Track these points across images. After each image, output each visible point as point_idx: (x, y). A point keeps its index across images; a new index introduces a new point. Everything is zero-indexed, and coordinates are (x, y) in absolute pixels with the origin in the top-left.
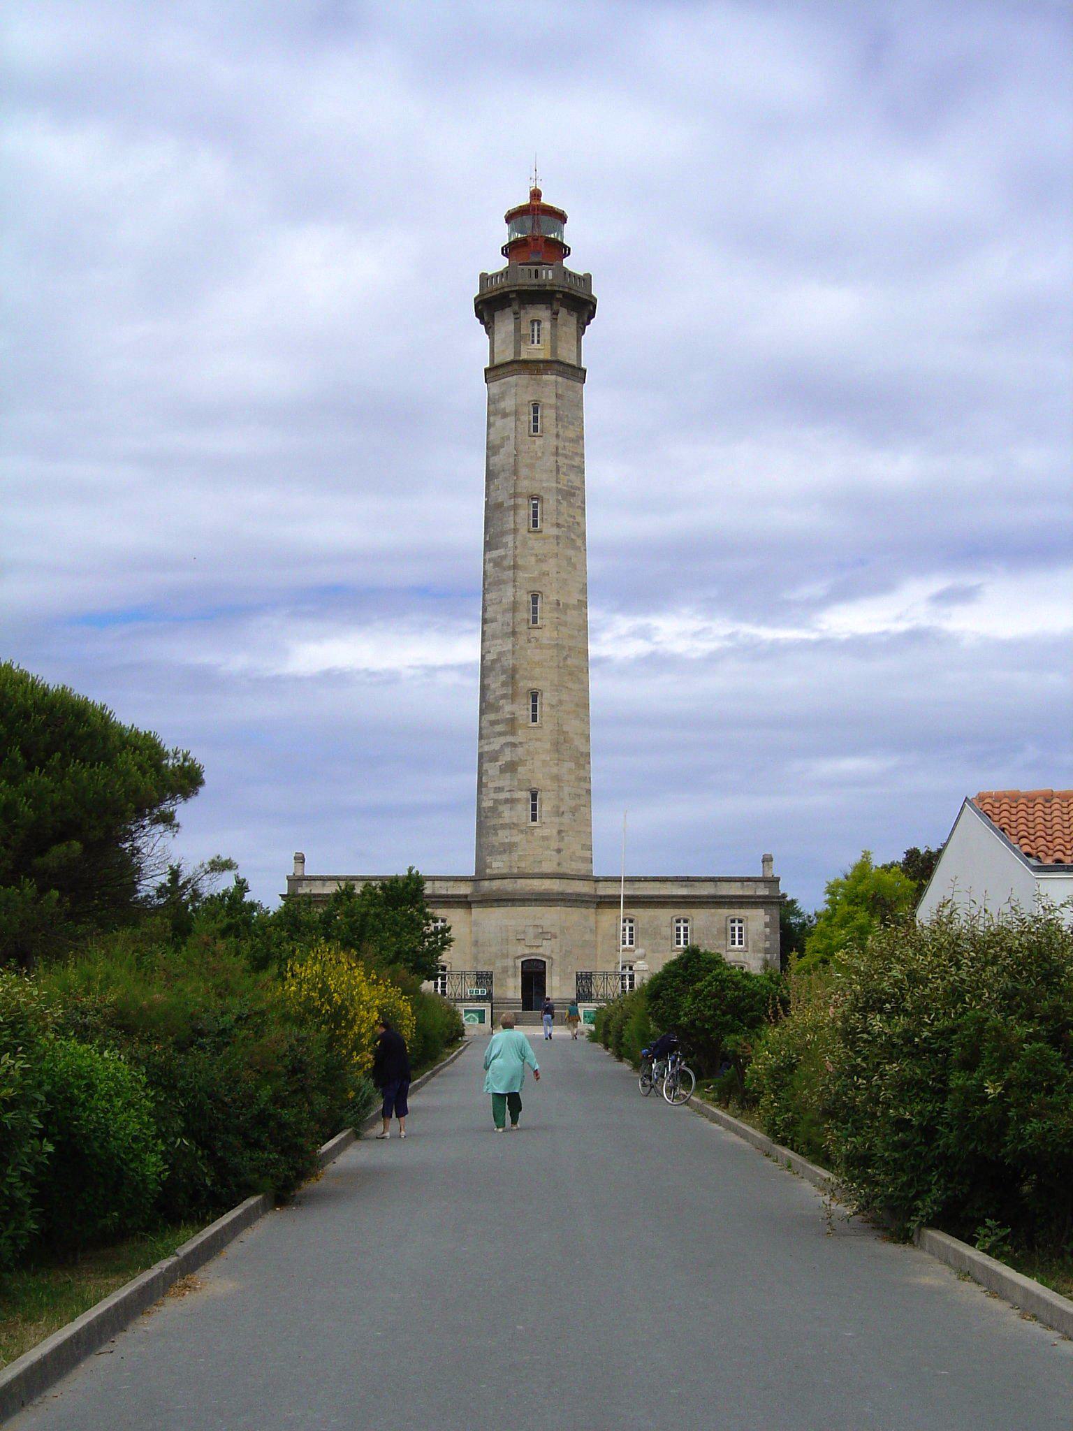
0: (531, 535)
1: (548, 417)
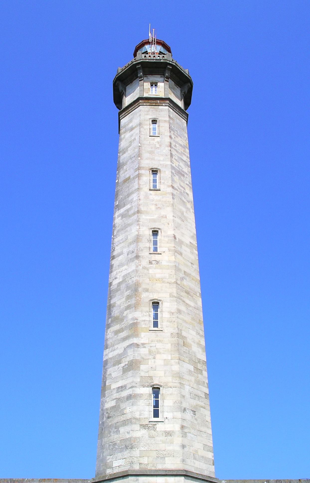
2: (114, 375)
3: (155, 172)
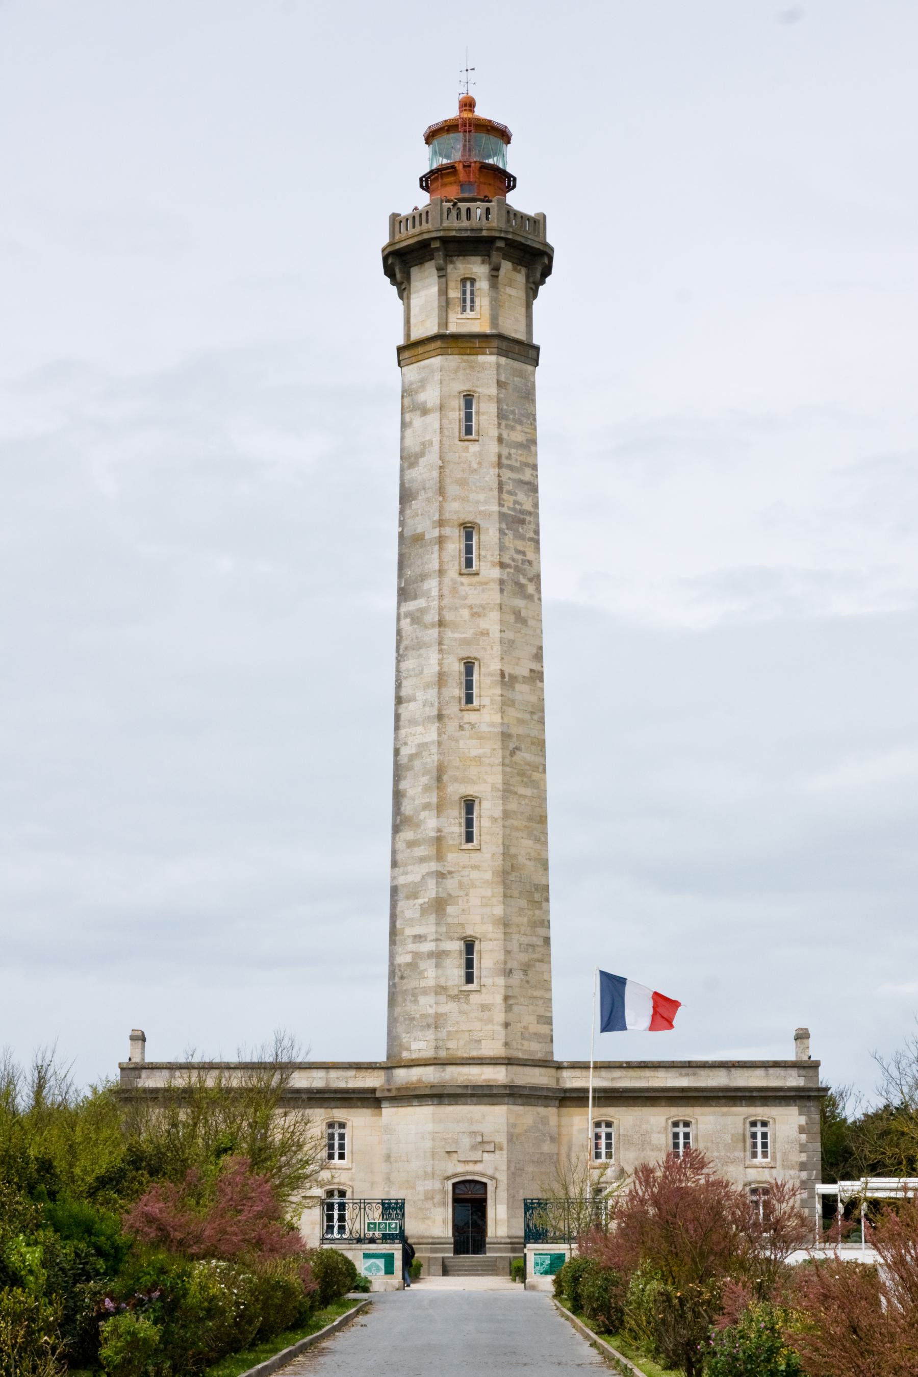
0: (464, 579)
1: (486, 415)
2: (408, 914)
3: (469, 530)
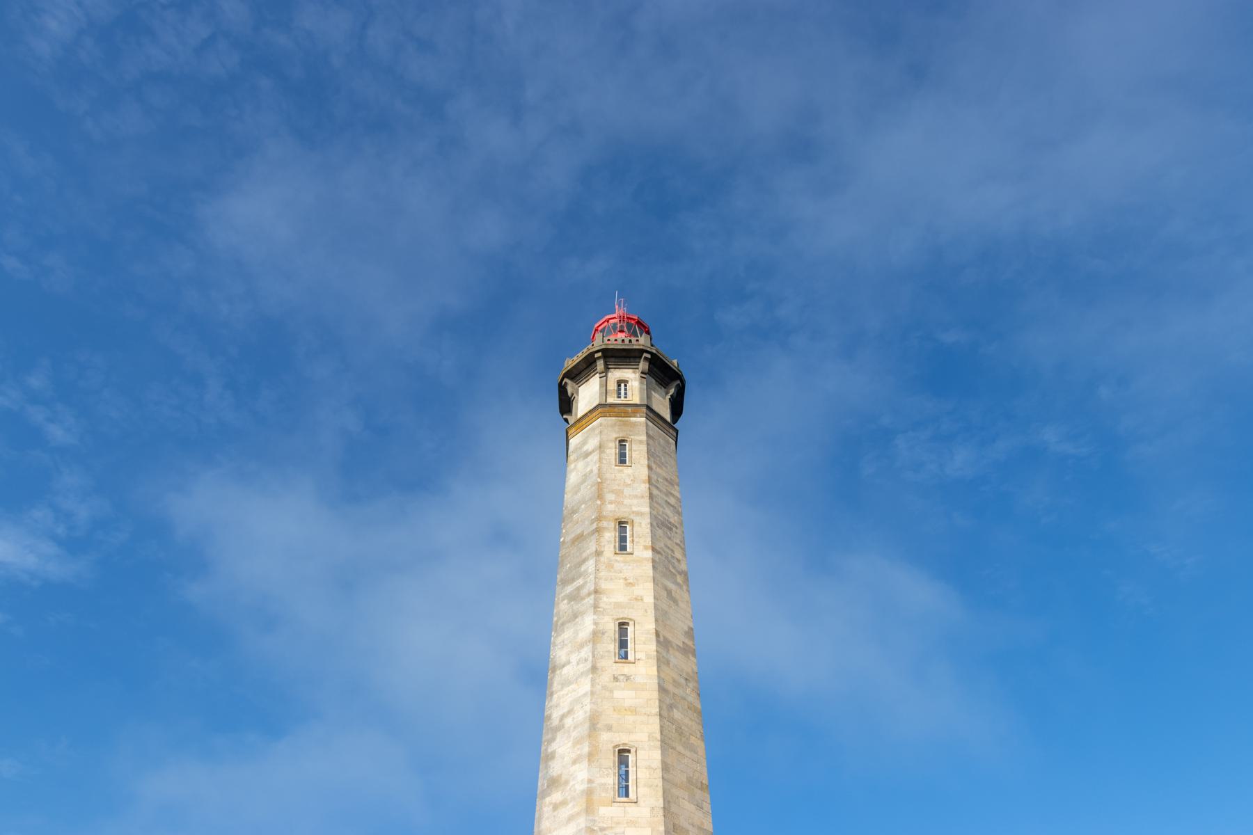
0: (619, 558)
